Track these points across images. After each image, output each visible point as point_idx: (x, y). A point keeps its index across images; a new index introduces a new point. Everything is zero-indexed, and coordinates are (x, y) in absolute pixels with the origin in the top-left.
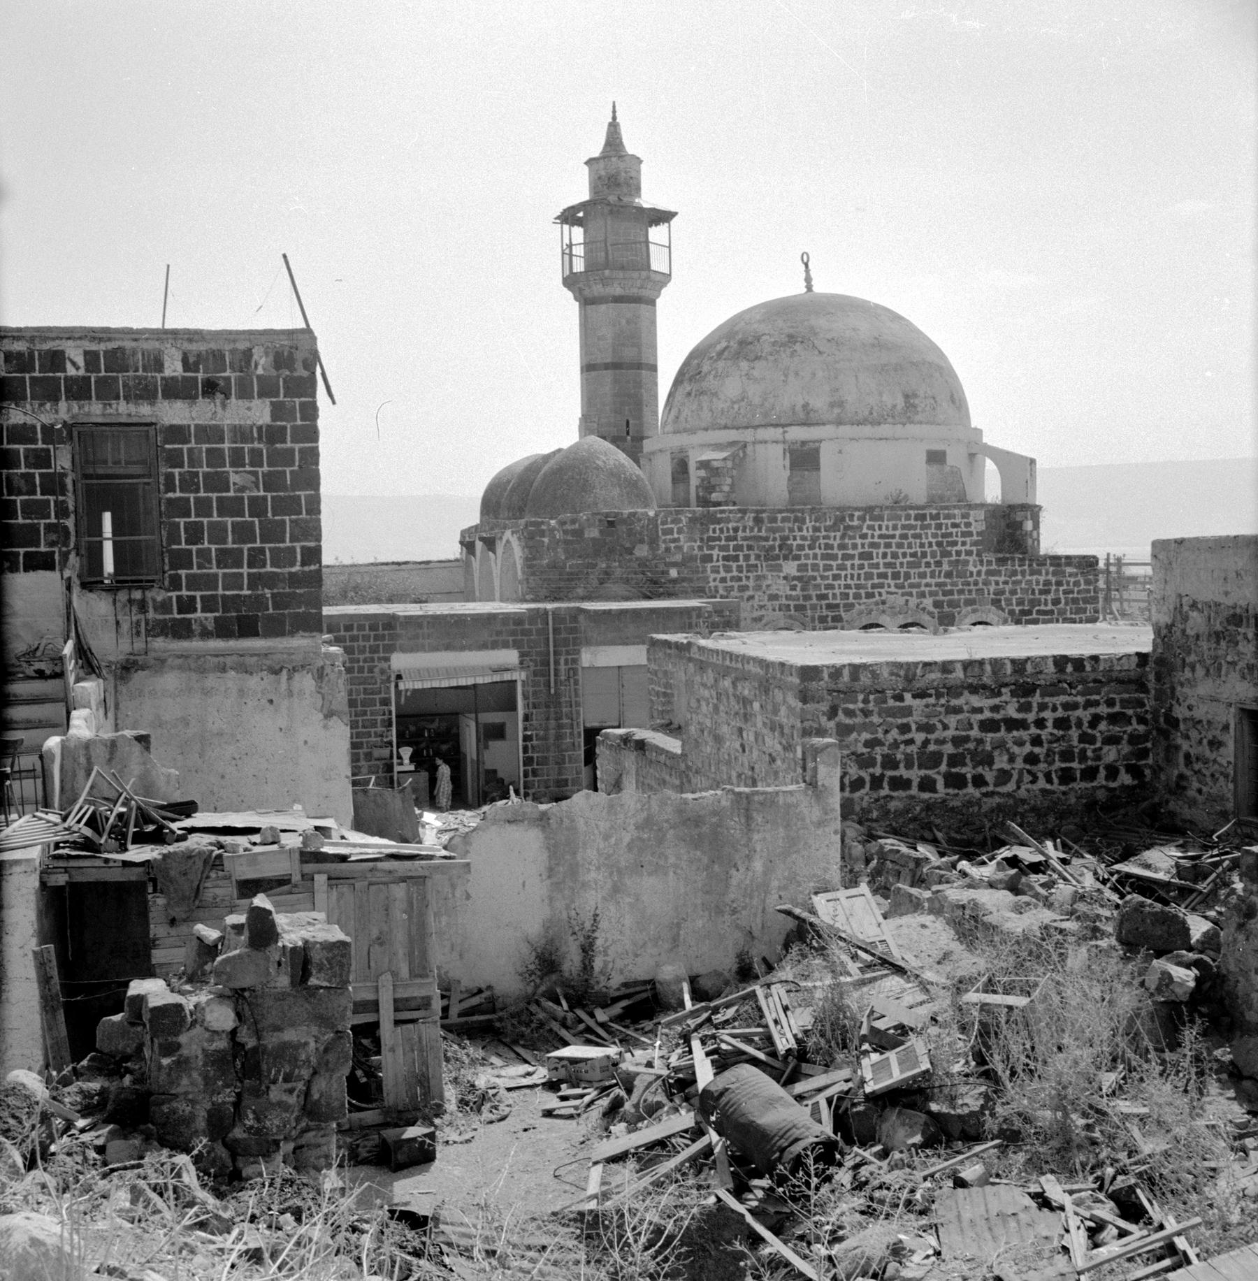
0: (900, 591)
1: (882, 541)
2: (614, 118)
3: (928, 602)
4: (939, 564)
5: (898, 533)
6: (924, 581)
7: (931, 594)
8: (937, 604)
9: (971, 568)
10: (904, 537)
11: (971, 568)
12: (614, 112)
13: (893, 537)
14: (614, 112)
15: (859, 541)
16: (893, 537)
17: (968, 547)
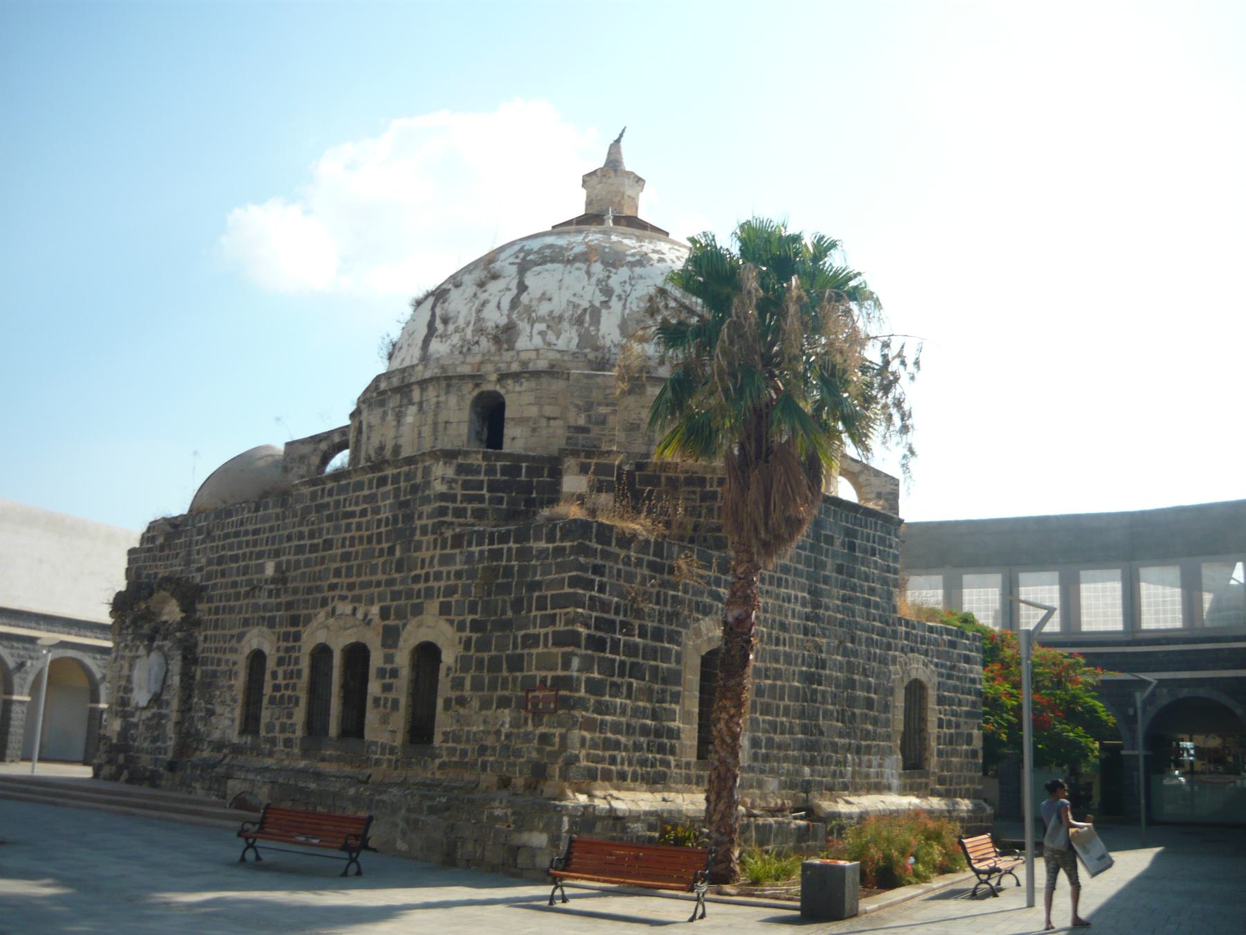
0: (350, 594)
1: (343, 522)
2: (618, 141)
3: (375, 610)
4: (391, 551)
5: (358, 509)
6: (374, 578)
7: (381, 597)
8: (384, 613)
9: (425, 554)
10: (363, 513)
11: (425, 554)
12: (621, 135)
13: (352, 515)
14: (621, 135)
15: (326, 525)
16: (352, 515)
17: (424, 522)
